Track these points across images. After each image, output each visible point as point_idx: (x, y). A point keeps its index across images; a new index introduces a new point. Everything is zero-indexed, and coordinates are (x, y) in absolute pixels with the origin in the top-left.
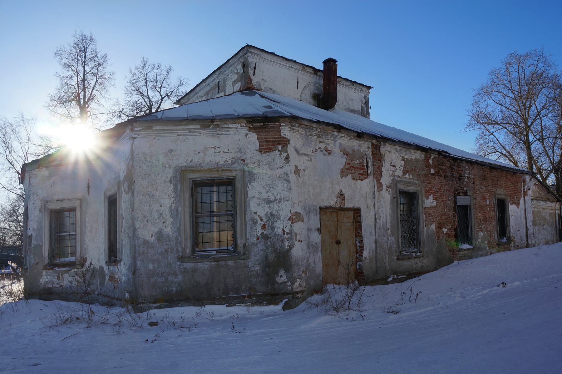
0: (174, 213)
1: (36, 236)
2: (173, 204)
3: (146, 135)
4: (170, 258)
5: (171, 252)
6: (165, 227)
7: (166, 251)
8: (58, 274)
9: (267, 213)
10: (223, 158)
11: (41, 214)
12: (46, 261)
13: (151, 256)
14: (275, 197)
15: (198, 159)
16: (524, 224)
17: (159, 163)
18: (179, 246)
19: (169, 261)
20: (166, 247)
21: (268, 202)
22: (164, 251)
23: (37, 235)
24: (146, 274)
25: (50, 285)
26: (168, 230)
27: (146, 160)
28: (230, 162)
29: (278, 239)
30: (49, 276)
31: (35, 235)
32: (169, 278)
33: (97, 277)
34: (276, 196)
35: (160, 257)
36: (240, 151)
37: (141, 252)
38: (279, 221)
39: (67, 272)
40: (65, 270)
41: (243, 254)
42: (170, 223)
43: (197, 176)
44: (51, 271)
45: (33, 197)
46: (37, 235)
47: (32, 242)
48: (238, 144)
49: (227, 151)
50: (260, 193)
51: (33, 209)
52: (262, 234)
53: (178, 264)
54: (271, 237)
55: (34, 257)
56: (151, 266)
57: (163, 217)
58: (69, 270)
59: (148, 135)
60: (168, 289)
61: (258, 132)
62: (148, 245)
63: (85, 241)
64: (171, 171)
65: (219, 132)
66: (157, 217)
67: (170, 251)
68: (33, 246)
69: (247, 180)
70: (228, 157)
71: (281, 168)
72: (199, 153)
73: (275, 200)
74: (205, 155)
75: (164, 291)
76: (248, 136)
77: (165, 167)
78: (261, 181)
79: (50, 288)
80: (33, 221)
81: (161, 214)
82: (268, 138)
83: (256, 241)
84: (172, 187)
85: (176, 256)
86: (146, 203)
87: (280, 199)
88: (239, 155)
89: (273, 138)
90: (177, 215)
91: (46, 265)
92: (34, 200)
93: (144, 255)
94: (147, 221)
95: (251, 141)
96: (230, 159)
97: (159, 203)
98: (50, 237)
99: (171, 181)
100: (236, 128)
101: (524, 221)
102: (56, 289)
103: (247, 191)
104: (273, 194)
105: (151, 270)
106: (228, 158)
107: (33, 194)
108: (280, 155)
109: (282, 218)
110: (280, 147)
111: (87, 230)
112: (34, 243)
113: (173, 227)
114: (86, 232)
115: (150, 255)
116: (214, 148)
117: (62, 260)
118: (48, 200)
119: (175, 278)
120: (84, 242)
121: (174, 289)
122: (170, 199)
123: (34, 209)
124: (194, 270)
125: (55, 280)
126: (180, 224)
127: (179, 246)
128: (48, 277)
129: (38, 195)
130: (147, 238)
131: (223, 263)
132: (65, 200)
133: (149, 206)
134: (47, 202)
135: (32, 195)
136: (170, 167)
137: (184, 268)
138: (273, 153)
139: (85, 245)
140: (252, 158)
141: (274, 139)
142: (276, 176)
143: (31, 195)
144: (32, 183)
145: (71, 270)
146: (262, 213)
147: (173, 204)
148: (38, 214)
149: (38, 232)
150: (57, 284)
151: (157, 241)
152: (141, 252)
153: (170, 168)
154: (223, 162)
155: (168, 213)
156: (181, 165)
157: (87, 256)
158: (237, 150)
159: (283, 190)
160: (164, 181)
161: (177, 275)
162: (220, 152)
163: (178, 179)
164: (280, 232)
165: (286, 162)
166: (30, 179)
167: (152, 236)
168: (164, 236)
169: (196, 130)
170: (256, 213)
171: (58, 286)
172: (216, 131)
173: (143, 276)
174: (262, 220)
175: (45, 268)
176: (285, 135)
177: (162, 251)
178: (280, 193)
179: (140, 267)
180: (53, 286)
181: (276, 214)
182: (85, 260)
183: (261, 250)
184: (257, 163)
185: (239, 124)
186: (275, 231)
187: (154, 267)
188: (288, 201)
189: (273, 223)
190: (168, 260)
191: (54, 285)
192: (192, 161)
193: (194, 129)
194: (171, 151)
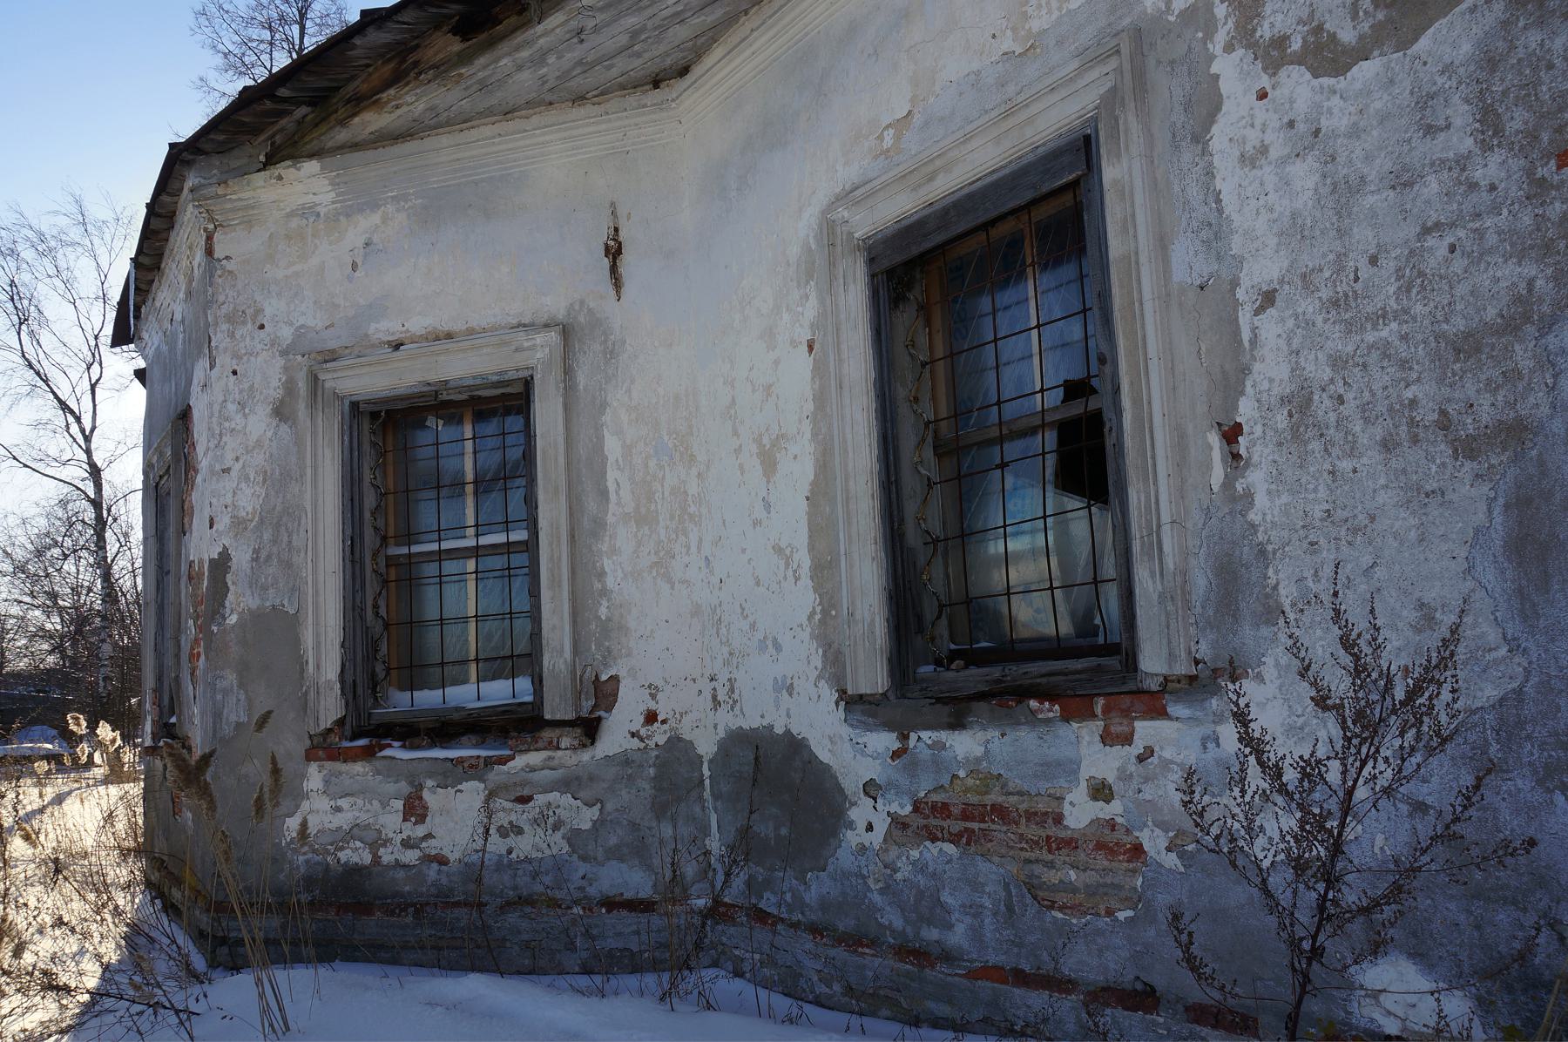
1: (255, 559)
8: (411, 783)
11: (284, 428)
12: (330, 708)
23: (263, 555)
25: (356, 854)
31: (248, 556)
33: (701, 798)
39: (473, 769)
40: (460, 761)
44: (358, 767)
46: (263, 555)
47: (231, 597)
51: (232, 407)
55: (241, 685)
58: (489, 762)
63: (602, 575)
79: (355, 871)
80: (234, 473)
91: (329, 731)
92: (237, 356)
98: (353, 562)
102: (401, 874)
107: (230, 319)
111: (612, 507)
112: (240, 601)
114: (610, 519)
117: (428, 698)
118: (332, 345)
120: (598, 586)
123: (242, 405)
125: (392, 821)
128: (343, 803)
129: (262, 327)
132: (449, 336)
134: (331, 356)
135: (224, 327)
139: (605, 603)
143: (217, 324)
144: (227, 258)
145: (503, 761)
148: (269, 434)
149: (267, 536)
150: (407, 844)
157: (622, 674)
166: (209, 238)
171: (411, 857)
175: (323, 748)
180: (376, 859)
182: (606, 693)
191: (382, 851)
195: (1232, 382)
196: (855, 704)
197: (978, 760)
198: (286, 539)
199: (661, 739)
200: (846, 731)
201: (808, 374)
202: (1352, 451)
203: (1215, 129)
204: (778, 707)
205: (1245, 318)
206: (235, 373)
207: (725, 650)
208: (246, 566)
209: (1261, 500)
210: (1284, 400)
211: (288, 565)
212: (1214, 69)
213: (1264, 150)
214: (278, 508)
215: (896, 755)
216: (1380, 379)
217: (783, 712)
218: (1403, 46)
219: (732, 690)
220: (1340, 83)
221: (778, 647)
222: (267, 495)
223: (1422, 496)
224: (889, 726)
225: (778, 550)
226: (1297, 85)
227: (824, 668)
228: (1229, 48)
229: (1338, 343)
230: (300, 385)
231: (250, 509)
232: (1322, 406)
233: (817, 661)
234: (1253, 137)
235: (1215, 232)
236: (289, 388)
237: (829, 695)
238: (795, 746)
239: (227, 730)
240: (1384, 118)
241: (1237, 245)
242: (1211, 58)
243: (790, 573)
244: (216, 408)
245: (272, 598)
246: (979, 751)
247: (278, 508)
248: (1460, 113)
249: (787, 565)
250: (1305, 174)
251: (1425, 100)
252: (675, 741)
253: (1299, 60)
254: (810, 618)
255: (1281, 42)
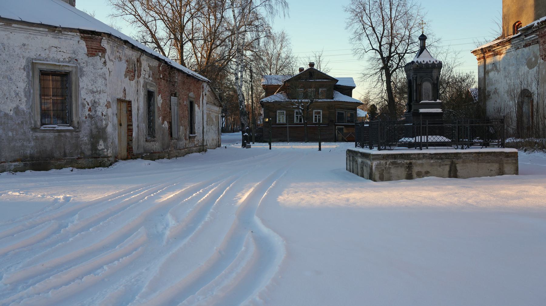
0: (27, 94)
2: (27, 87)
3: (5, 29)
4: (25, 128)
5: (26, 124)
6: (21, 104)
7: (22, 123)
9: (92, 100)
10: (62, 56)
13: (11, 126)
14: (97, 89)
15: (45, 54)
16: (202, 123)
17: (15, 53)
18: (32, 120)
19: (24, 130)
20: (22, 119)
21: (93, 92)
22: (20, 122)
24: (7, 140)
26: (23, 107)
27: (5, 50)
28: (67, 60)
29: (99, 119)
32: (25, 143)
34: (98, 88)
35: (17, 127)
36: (74, 53)
37: (3, 122)
38: (99, 106)
41: (77, 128)
42: (25, 102)
43: (44, 68)
48: (73, 47)
49: (66, 52)
50: (87, 85)
52: (89, 114)
53: (31, 133)
54: (94, 118)
56: (10, 134)
57: (18, 96)
59: (6, 29)
60: (24, 152)
61: (86, 40)
62: (8, 117)
64: (25, 61)
65: (60, 36)
66: (14, 96)
67: (25, 123)
69: (79, 75)
70: (66, 56)
71: (101, 69)
72: (45, 50)
73: (97, 91)
74: (49, 52)
75: (20, 153)
76: (80, 42)
77: (20, 57)
78: (88, 76)
81: (18, 94)
82: (92, 46)
83: (85, 120)
84: (25, 73)
85: (29, 127)
86: (5, 84)
87: (100, 91)
88: (74, 56)
89: (95, 47)
90: (30, 96)
93: (5, 125)
94: (7, 98)
95: (82, 47)
96: (67, 58)
97: (16, 85)
99: (24, 69)
100: (73, 35)
101: (202, 120)
103: (79, 83)
104: (96, 87)
105: (10, 137)
106: (66, 57)
108: (101, 59)
109: (101, 104)
110: (100, 54)
113: (27, 104)
115: (10, 125)
116: (56, 48)
119: (29, 143)
121: (29, 152)
122: (24, 83)
124: (43, 138)
126: (32, 104)
127: (32, 120)
130: (8, 112)
131: (63, 134)
133: (8, 87)
136: (23, 57)
137: (35, 136)
138: (96, 57)
140: (82, 59)
141: (97, 47)
142: (98, 75)
146: (89, 100)
147: (27, 87)
151: (15, 114)
152: (3, 122)
153: (24, 58)
154: (62, 60)
155: (23, 93)
156: (32, 57)
158: (72, 52)
159: (102, 85)
160: (19, 68)
161: (30, 141)
162: (60, 51)
163: (30, 68)
164: (100, 114)
165: (104, 65)
167: (11, 110)
168: (20, 111)
169: (44, 32)
170: (85, 99)
172: (58, 35)
173: (4, 141)
174: (88, 105)
176: (104, 45)
177: (19, 123)
178: (100, 87)
179: (2, 134)
181: (98, 101)
183: (88, 126)
184: (85, 63)
185: (76, 33)
186: (97, 113)
187: (13, 134)
188: (105, 93)
189: (95, 107)
190: (23, 130)
192: (40, 55)
193: (43, 31)
194: (24, 45)
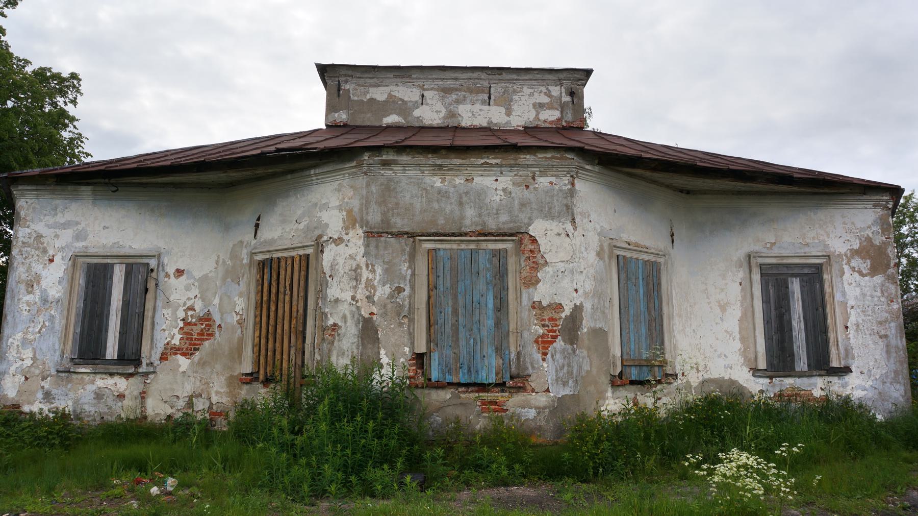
1: (593, 309)
11: (601, 262)
23: (595, 307)
30: (619, 399)
31: (590, 307)
45: (582, 221)
46: (595, 307)
47: (584, 322)
51: (583, 249)
68: (585, 330)
80: (584, 274)
112: (587, 324)
123: (586, 249)
128: (617, 401)
148: (596, 263)
149: (596, 301)
195: (847, 319)
196: (755, 371)
197: (792, 384)
198: (602, 303)
199: (685, 381)
200: (753, 378)
201: (740, 291)
202: (866, 335)
203: (844, 277)
204: (726, 372)
205: (848, 309)
206: (583, 236)
207: (703, 357)
208: (589, 310)
209: (851, 339)
210: (855, 324)
211: (604, 313)
212: (844, 267)
213: (852, 284)
214: (600, 291)
215: (770, 383)
216: (869, 325)
217: (728, 374)
218: (872, 277)
219: (706, 367)
220: (863, 278)
221: (725, 356)
222: (595, 285)
223: (875, 343)
224: (767, 377)
225: (726, 332)
226: (856, 275)
227: (744, 362)
228: (846, 264)
229: (863, 317)
230: (605, 248)
231: (589, 289)
232: (861, 326)
233: (742, 360)
234: (850, 281)
235: (844, 294)
236: (601, 247)
237: (746, 369)
238: (733, 382)
239: (584, 373)
240: (869, 286)
241: (847, 297)
242: (843, 265)
243: (731, 338)
244: (578, 247)
245: (599, 325)
246: (793, 382)
247: (600, 291)
248: (879, 291)
249: (730, 336)
250: (858, 290)
251: (875, 286)
252: (688, 382)
253: (857, 272)
254: (739, 350)
255: (854, 268)
